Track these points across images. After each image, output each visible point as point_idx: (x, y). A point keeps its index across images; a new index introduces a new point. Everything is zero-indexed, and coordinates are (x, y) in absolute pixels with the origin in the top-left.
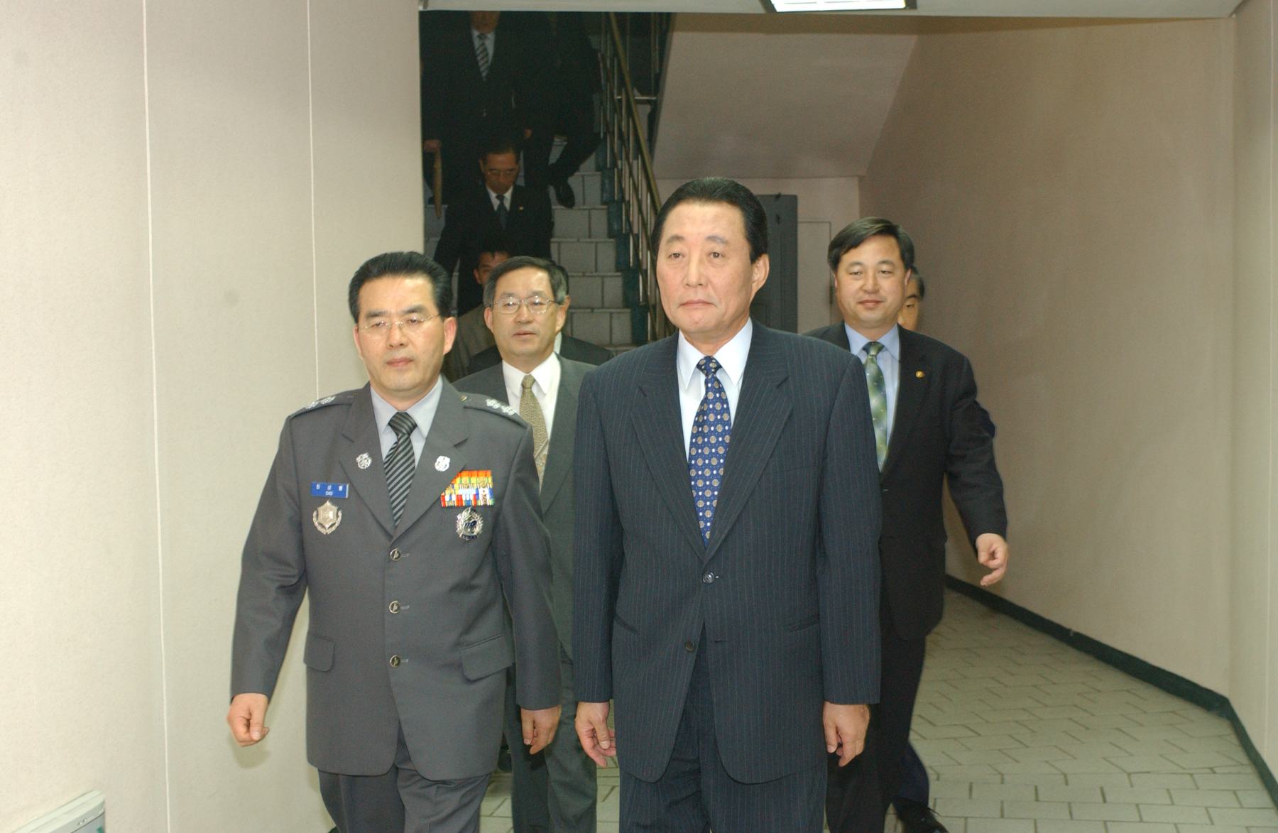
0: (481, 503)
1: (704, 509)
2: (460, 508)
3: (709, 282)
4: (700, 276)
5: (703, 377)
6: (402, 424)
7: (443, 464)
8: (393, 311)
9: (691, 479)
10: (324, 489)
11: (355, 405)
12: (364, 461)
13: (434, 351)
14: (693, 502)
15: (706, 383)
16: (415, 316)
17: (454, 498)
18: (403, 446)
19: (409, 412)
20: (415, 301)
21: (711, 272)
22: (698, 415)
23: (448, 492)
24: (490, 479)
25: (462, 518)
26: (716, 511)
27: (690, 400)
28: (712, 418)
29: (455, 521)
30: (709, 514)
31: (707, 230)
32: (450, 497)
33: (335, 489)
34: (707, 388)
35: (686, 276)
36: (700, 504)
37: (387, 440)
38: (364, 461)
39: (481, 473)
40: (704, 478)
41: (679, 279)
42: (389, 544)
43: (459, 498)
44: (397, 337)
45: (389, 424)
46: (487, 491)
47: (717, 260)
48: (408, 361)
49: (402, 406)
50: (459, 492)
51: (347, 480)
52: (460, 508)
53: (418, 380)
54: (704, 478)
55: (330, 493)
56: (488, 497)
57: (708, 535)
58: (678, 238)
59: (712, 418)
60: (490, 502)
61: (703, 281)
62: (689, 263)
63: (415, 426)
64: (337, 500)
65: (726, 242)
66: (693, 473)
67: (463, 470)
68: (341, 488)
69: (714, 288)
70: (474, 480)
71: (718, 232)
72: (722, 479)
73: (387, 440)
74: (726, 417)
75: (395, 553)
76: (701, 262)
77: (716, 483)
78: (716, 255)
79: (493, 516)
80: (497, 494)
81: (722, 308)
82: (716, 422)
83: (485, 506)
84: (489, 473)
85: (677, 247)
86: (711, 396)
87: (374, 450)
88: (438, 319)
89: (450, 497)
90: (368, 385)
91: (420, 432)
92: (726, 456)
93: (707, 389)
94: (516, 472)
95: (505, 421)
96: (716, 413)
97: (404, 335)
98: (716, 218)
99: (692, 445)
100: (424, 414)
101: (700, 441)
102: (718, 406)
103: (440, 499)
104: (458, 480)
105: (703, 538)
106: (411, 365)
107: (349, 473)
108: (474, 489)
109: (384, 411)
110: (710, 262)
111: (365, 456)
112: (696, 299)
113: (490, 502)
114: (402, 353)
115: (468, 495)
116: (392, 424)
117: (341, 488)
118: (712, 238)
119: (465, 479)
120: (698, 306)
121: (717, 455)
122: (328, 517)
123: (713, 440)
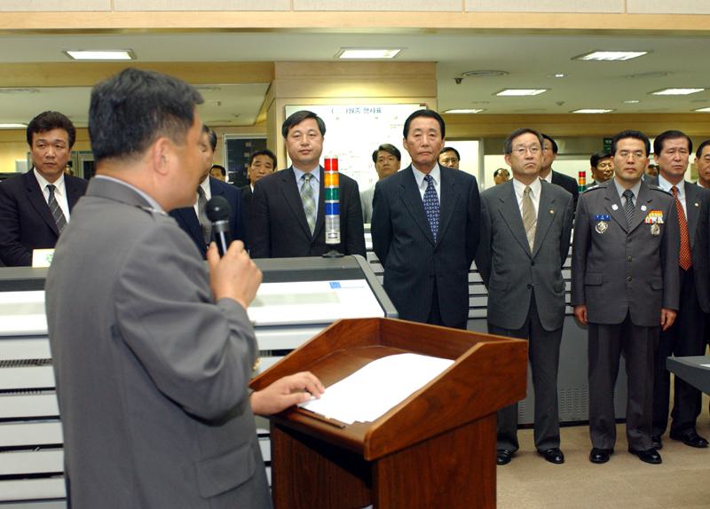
6: (628, 194)
7: (644, 208)
12: (615, 207)
25: (653, 227)
29: (650, 228)
33: (605, 217)
37: (623, 201)
38: (615, 207)
48: (634, 169)
63: (633, 195)
64: (606, 220)
73: (623, 201)
79: (663, 227)
80: (665, 220)
87: (619, 204)
94: (672, 211)
103: (644, 220)
107: (608, 210)
108: (656, 217)
113: (662, 222)
115: (654, 219)
116: (624, 195)
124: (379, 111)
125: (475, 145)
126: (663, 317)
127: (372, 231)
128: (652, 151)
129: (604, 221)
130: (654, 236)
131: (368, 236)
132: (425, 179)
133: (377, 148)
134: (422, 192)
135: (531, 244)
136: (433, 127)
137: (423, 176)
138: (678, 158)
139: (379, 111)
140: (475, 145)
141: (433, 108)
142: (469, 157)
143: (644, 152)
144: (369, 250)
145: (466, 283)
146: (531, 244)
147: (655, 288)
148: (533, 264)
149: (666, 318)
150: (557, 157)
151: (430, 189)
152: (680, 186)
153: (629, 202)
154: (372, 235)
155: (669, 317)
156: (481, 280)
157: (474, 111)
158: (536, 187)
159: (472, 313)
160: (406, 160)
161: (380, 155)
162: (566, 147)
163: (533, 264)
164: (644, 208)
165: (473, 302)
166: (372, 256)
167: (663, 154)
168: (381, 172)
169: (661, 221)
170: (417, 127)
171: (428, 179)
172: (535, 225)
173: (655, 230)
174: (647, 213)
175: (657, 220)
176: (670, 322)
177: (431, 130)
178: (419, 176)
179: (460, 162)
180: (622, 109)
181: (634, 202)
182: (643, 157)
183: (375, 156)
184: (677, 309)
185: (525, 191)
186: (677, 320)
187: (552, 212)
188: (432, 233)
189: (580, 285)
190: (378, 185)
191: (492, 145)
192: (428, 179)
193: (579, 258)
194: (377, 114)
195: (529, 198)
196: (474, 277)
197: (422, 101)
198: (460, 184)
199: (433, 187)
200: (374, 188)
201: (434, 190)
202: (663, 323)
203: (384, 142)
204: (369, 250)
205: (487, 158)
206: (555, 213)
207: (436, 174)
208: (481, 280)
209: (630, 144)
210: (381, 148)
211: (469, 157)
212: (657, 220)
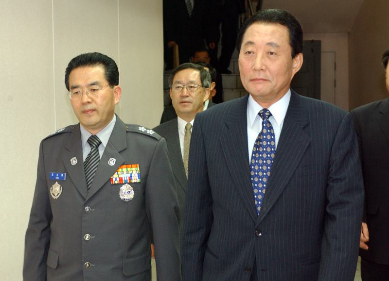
1: (257, 195)
2: (121, 183)
3: (267, 68)
4: (262, 64)
5: (261, 120)
6: (94, 141)
7: (112, 162)
8: (83, 85)
9: (251, 176)
10: (55, 175)
11: (71, 134)
13: (107, 104)
14: (252, 189)
15: (263, 123)
16: (94, 87)
17: (118, 179)
19: (97, 135)
21: (268, 63)
22: (257, 141)
23: (115, 175)
24: (138, 168)
26: (264, 196)
27: (253, 133)
28: (265, 143)
29: (118, 191)
30: (260, 197)
31: (267, 39)
32: (116, 178)
33: (60, 176)
34: (263, 126)
35: (254, 65)
36: (256, 191)
38: (74, 161)
39: (133, 165)
40: (258, 177)
41: (250, 65)
42: (84, 203)
43: (121, 179)
44: (86, 99)
45: (87, 141)
46: (137, 175)
47: (272, 56)
48: (94, 110)
49: (94, 132)
50: (120, 176)
54: (258, 177)
55: (58, 178)
56: (137, 178)
57: (259, 209)
58: (251, 43)
59: (265, 143)
60: (139, 181)
61: (264, 68)
62: (256, 57)
63: (100, 143)
64: (61, 182)
65: (278, 46)
66: (252, 173)
67: (123, 164)
68: (62, 175)
69: (270, 72)
70: (129, 169)
71: (274, 40)
72: (269, 178)
73: (86, 150)
74: (272, 143)
75: (87, 208)
76: (263, 57)
77: (265, 180)
78: (271, 53)
79: (142, 189)
80: (144, 177)
81: (274, 83)
82: (267, 146)
83: (135, 183)
85: (250, 49)
86: (265, 131)
88: (108, 88)
89: (116, 178)
90: (79, 124)
91: (103, 145)
92: (272, 165)
93: (263, 127)
95: (149, 138)
96: (267, 141)
98: (273, 33)
99: (253, 157)
100: (104, 136)
101: (257, 156)
102: (269, 137)
104: (120, 170)
105: (257, 210)
106: (94, 112)
107: (67, 167)
108: (131, 173)
109: (86, 135)
110: (268, 57)
111: (75, 158)
112: (259, 78)
113: (139, 181)
114: (89, 107)
116: (89, 141)
117: (62, 175)
118: (270, 44)
119: (125, 170)
120: (261, 81)
121: (266, 164)
122: (56, 190)
123: (265, 156)
130: (124, 201)
169: (136, 179)
173: (127, 193)
174: (115, 169)
175: (130, 178)
212: (130, 178)
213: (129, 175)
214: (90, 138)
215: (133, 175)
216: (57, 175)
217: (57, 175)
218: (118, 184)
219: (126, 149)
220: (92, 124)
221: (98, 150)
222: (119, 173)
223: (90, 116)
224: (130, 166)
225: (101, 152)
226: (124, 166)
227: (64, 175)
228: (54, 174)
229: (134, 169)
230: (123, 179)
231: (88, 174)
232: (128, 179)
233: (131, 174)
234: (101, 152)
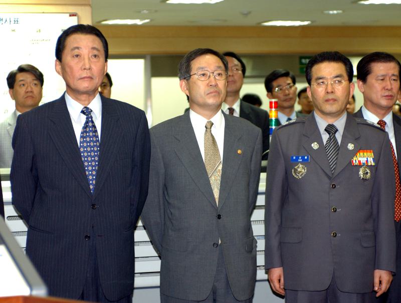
0: (369, 164)
10: (297, 158)
12: (315, 146)
13: (346, 96)
17: (357, 162)
18: (332, 138)
19: (334, 124)
20: (337, 72)
23: (355, 159)
33: (303, 158)
37: (325, 137)
38: (315, 146)
43: (359, 162)
44: (329, 90)
45: (325, 130)
46: (371, 159)
48: (335, 100)
50: (360, 159)
51: (308, 154)
52: (360, 165)
53: (339, 109)
55: (301, 160)
56: (372, 162)
60: (373, 164)
63: (337, 130)
64: (304, 162)
67: (360, 149)
68: (306, 158)
73: (325, 137)
83: (371, 165)
84: (372, 151)
87: (320, 141)
91: (339, 133)
97: (333, 88)
100: (340, 123)
103: (351, 162)
106: (336, 102)
108: (365, 158)
109: (322, 123)
113: (373, 164)
114: (330, 97)
115: (363, 160)
117: (306, 158)
119: (361, 154)
124: (16, 21)
125: (138, 66)
126: (377, 281)
127: (12, 177)
128: (355, 73)
129: (301, 163)
131: (6, 185)
132: (83, 112)
133: (15, 68)
134: (78, 129)
135: (216, 193)
136: (95, 46)
137: (81, 107)
138: (389, 87)
139: (16, 21)
140: (138, 66)
141: (87, 21)
142: (129, 80)
143: (346, 77)
144: (8, 203)
145: (130, 243)
146: (216, 193)
147: (365, 245)
148: (219, 217)
149: (380, 282)
150: (245, 80)
151: (89, 124)
152: (388, 119)
153: (332, 138)
154: (12, 183)
155: (382, 279)
156: (149, 240)
157: (139, 22)
158: (219, 121)
159: (139, 281)
160: (53, 89)
161: (20, 77)
162: (254, 68)
163: (219, 217)
164: (351, 147)
165: (139, 267)
166: (9, 210)
167: (371, 79)
168: (18, 105)
169: (371, 162)
170: (76, 45)
171: (86, 112)
172: (220, 167)
174: (354, 153)
175: (367, 161)
176: (385, 287)
177: (94, 48)
178: (74, 108)
179: (113, 88)
180: (322, 21)
181: (339, 141)
182: (345, 83)
183: (12, 80)
184: (394, 271)
185: (206, 127)
186: (393, 284)
187: (239, 152)
188: (87, 180)
189: (275, 243)
190: (20, 120)
191: (169, 63)
192: (86, 112)
193: (275, 207)
194: (14, 26)
195: (210, 131)
196: (140, 235)
197: (73, 9)
198: (122, 118)
199: (92, 122)
200: (13, 123)
201: (94, 126)
202: (376, 289)
203: (24, 62)
204: (8, 203)
205: (157, 82)
206: (243, 153)
207: (96, 105)
208: (149, 240)
209: (328, 70)
210: (21, 70)
211: (129, 80)
212: (367, 161)
213: (365, 159)
214: (328, 126)
215: (369, 159)
216: (300, 158)
217: (300, 158)
218: (356, 166)
219: (359, 137)
220: (328, 112)
221: (335, 138)
222: (358, 156)
223: (332, 104)
224: (365, 151)
225: (339, 137)
226: (360, 151)
227: (308, 157)
228: (296, 157)
229: (369, 154)
230: (362, 162)
231: (336, 154)
232: (365, 162)
233: (367, 158)
234: (339, 137)
